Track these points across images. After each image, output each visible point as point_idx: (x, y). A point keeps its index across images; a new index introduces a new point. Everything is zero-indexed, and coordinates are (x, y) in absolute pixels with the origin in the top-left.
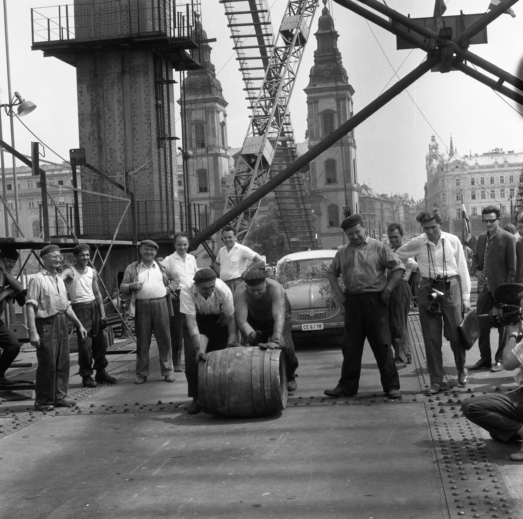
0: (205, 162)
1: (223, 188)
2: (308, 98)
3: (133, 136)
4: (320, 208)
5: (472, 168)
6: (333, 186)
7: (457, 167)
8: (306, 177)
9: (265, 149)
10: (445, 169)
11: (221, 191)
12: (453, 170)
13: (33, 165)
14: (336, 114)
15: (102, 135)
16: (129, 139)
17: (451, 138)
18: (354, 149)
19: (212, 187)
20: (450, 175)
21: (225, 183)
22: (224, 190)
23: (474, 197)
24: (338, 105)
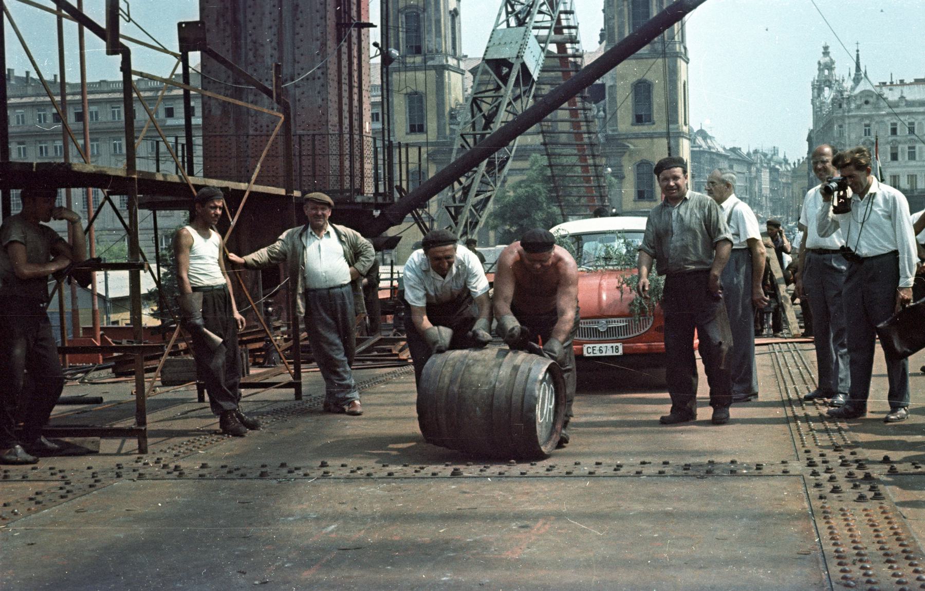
0: (420, 80)
1: (452, 126)
3: (295, 18)
4: (622, 166)
5: (891, 105)
6: (644, 129)
7: (867, 102)
8: (599, 111)
9: (527, 51)
10: (845, 106)
11: (448, 132)
12: (859, 107)
13: (109, 37)
15: (241, 17)
16: (287, 23)
17: (858, 51)
18: (685, 64)
19: (432, 125)
20: (854, 117)
21: (456, 118)
23: (894, 157)
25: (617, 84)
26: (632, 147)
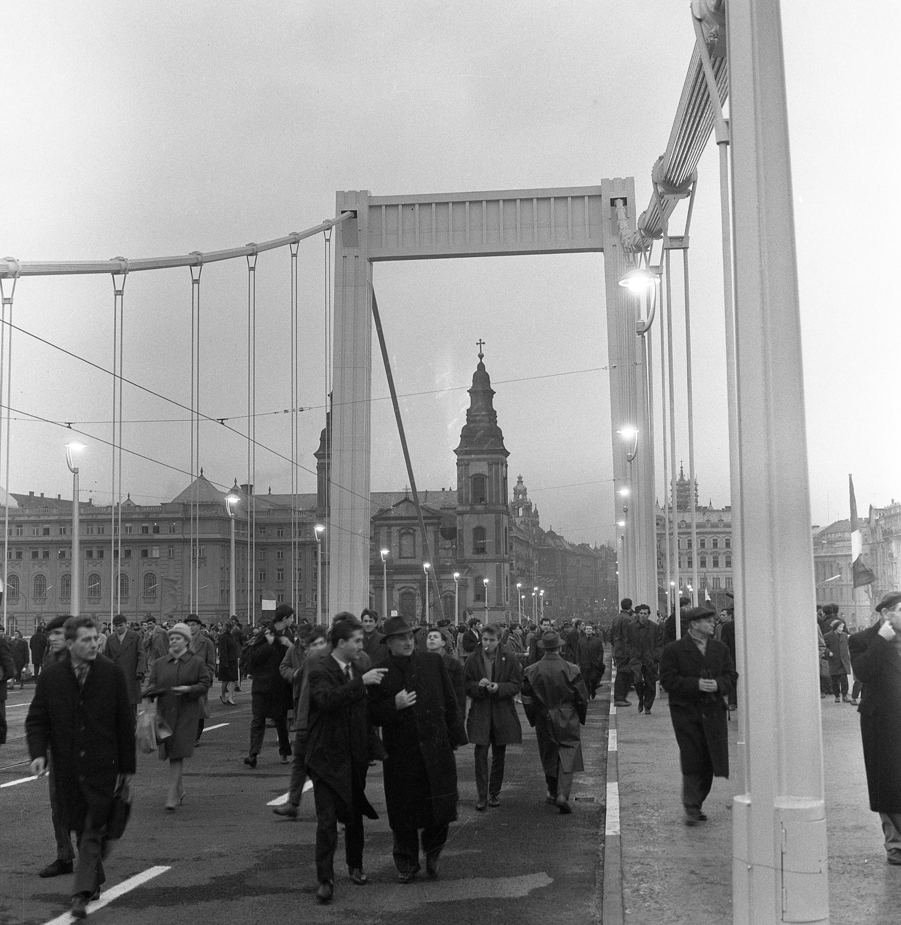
2: (458, 460)
6: (481, 557)
8: (452, 545)
17: (682, 467)
24: (490, 470)
26: (472, 567)
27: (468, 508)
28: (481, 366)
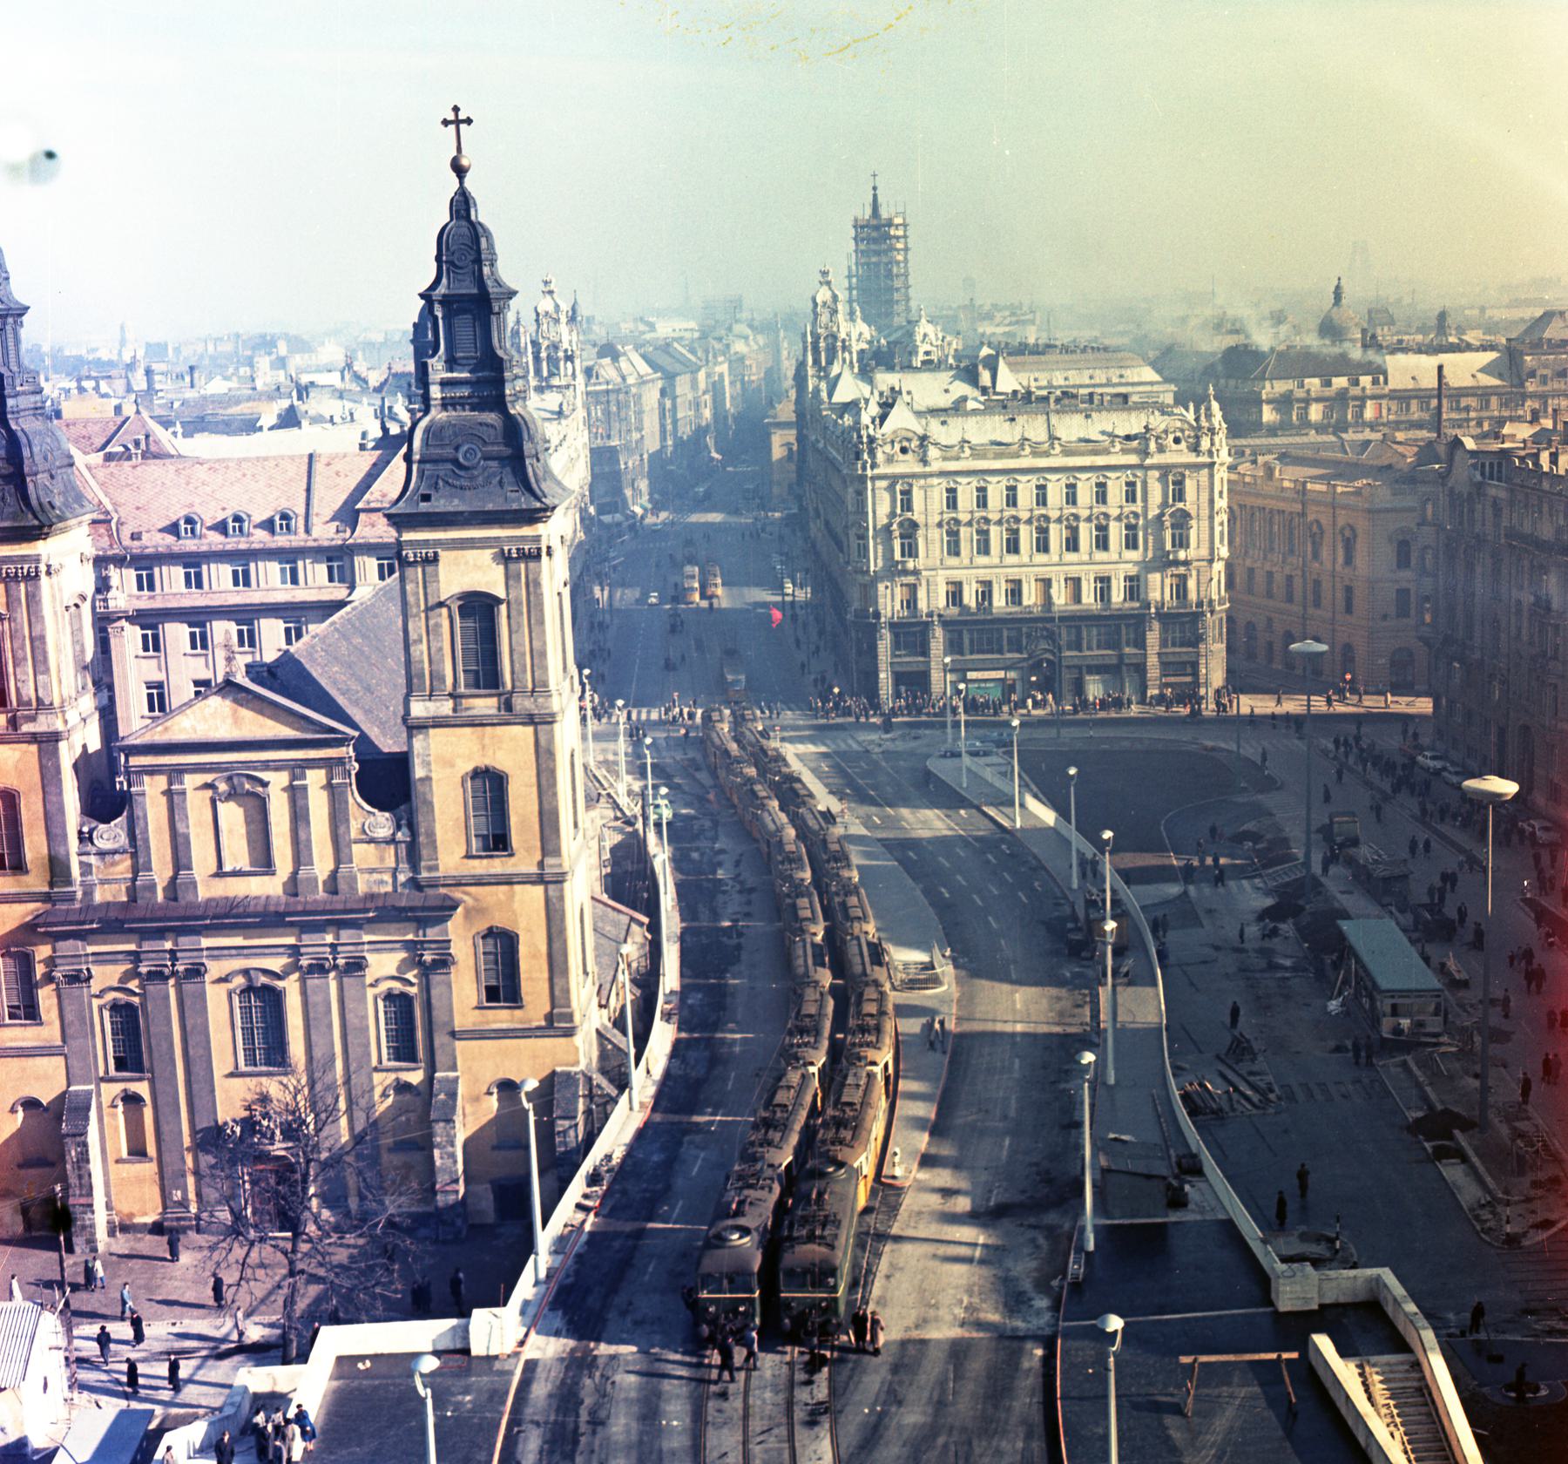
1: (84, 858)
6: (497, 866)
7: (904, 450)
12: (890, 459)
14: (503, 607)
17: (875, 188)
21: (91, 839)
22: (90, 865)
25: (434, 775)
27: (446, 707)
28: (462, 205)
